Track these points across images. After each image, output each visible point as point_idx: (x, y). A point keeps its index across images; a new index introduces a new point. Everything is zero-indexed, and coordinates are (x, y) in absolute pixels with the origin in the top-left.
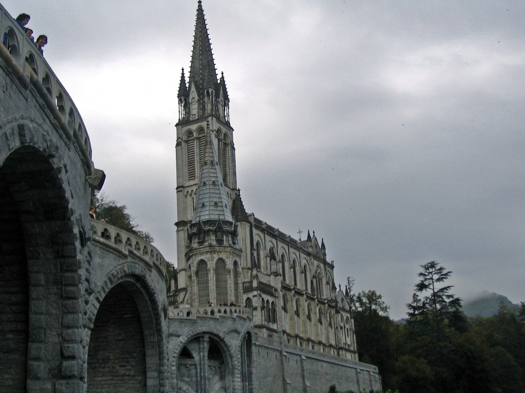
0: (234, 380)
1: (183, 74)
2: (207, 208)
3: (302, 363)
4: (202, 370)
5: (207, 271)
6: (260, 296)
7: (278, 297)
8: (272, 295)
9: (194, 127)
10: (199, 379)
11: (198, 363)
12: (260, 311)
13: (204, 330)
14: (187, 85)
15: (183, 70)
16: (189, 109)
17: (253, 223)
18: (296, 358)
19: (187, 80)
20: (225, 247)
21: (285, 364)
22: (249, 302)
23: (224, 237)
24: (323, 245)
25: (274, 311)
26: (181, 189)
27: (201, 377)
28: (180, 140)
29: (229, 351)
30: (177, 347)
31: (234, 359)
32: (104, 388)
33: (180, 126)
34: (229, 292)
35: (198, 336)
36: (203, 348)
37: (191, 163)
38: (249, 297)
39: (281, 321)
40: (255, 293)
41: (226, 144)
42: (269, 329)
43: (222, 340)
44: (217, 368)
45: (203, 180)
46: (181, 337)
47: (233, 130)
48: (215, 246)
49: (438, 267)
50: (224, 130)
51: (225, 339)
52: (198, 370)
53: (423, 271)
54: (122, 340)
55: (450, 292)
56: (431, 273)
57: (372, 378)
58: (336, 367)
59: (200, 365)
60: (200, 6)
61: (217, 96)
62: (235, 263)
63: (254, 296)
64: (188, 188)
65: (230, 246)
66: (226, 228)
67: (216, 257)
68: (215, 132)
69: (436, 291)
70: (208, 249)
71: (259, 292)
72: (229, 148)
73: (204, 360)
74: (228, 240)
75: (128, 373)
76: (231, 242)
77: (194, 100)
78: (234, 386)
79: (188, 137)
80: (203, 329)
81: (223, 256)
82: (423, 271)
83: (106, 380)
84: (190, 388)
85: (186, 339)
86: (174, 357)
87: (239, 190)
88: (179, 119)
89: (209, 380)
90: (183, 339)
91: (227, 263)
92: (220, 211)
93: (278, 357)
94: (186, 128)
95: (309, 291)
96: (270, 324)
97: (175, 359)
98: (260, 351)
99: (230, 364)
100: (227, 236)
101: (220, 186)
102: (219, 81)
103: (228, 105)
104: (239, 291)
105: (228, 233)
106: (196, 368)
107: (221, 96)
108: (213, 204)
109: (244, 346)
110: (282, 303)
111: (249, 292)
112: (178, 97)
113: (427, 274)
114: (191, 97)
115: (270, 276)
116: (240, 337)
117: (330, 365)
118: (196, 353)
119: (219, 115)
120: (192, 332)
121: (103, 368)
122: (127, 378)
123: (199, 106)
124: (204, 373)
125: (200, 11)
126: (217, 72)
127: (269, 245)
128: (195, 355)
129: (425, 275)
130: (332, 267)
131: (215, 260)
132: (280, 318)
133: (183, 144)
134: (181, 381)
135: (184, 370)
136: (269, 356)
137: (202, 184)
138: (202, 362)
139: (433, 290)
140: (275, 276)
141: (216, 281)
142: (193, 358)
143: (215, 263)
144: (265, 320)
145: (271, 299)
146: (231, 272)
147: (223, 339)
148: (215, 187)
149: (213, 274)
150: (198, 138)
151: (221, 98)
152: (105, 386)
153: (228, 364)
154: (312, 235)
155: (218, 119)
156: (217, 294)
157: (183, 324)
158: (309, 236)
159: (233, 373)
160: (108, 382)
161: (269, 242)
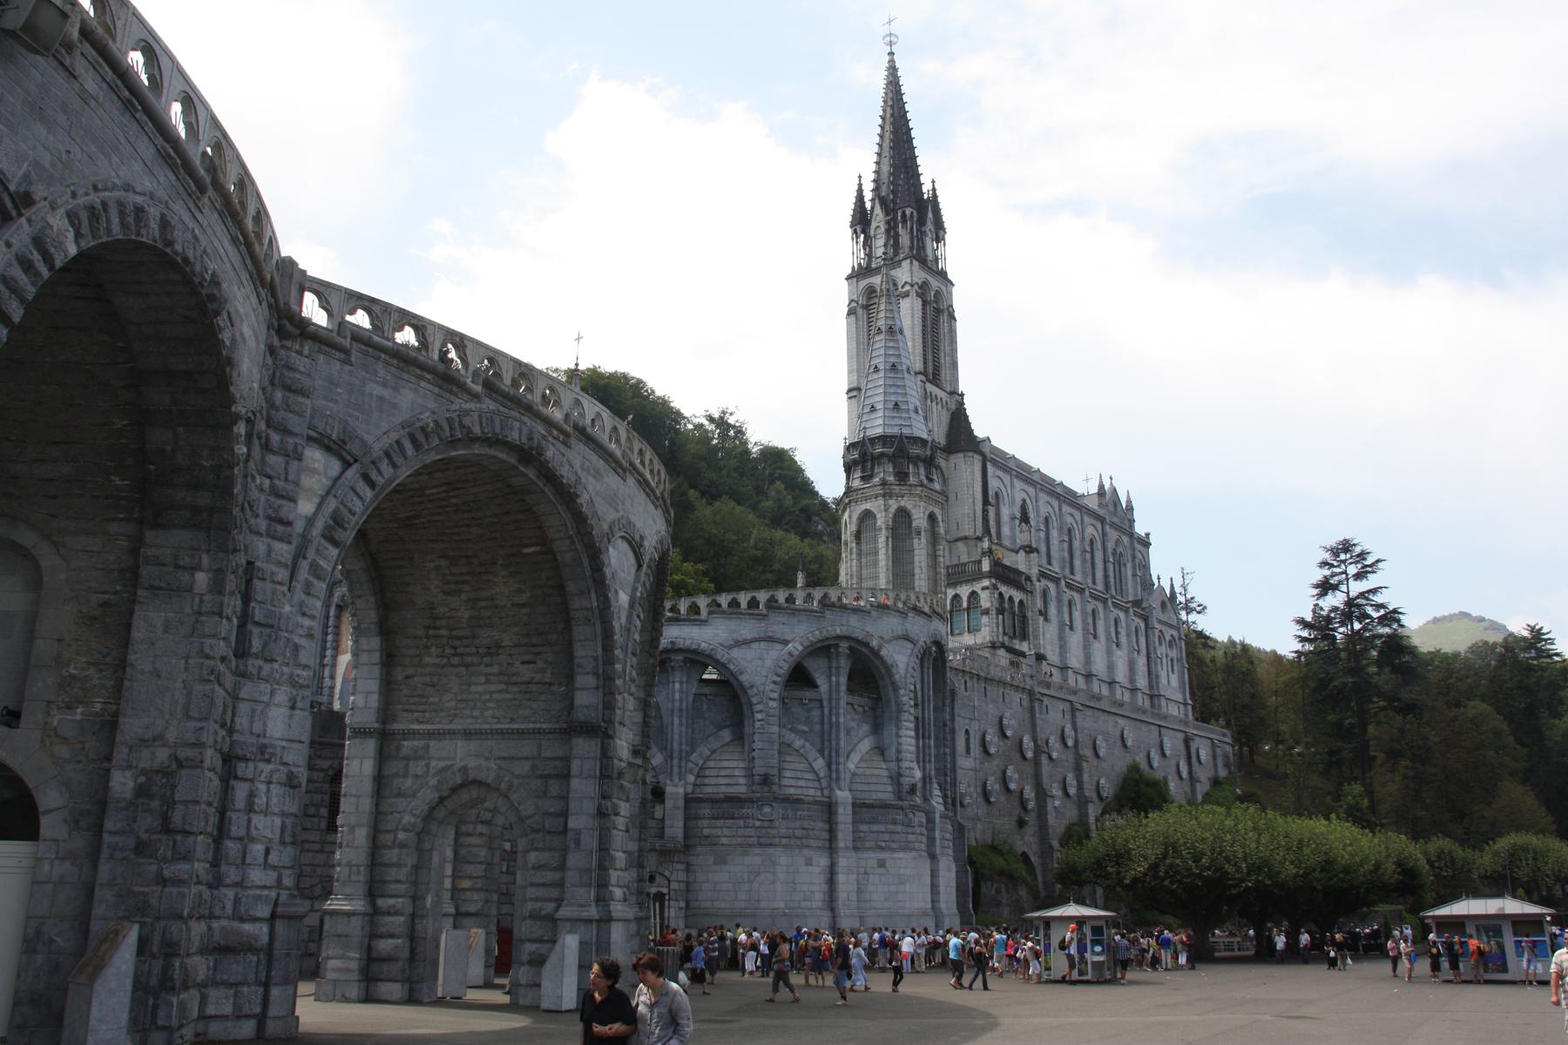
0: (900, 734)
1: (860, 185)
2: (880, 414)
3: (1073, 716)
4: (834, 711)
5: (876, 529)
6: (995, 587)
7: (1031, 592)
8: (1020, 587)
9: (876, 280)
10: (826, 727)
11: (825, 696)
12: (994, 616)
13: (838, 631)
14: (868, 205)
15: (860, 177)
16: (871, 247)
17: (989, 456)
18: (1061, 706)
19: (868, 195)
20: (911, 485)
21: (1037, 715)
22: (975, 599)
23: (911, 466)
24: (1129, 502)
25: (1024, 619)
26: (854, 393)
27: (830, 724)
28: (854, 304)
29: (891, 675)
30: (782, 663)
31: (902, 692)
32: (488, 709)
33: (855, 280)
34: (917, 571)
35: (826, 643)
36: (838, 668)
38: (975, 589)
39: (1036, 637)
40: (986, 583)
41: (938, 311)
42: (1010, 650)
43: (876, 653)
44: (867, 709)
45: (874, 362)
46: (790, 645)
47: (953, 285)
48: (891, 484)
49: (1358, 550)
50: (935, 283)
51: (883, 652)
52: (826, 711)
53: (1327, 556)
54: (524, 605)
55: (1378, 598)
56: (1344, 562)
57: (1218, 751)
58: (1143, 726)
59: (830, 700)
60: (892, 61)
61: (922, 222)
62: (932, 518)
63: (983, 589)
65: (922, 485)
66: (915, 451)
67: (893, 505)
68: (916, 287)
69: (1352, 594)
70: (879, 490)
71: (993, 581)
72: (944, 318)
73: (838, 691)
74: (918, 474)
75: (538, 677)
76: (923, 477)
78: (899, 744)
79: (869, 299)
80: (835, 630)
81: (906, 503)
82: (1327, 556)
83: (491, 693)
84: (807, 744)
85: (800, 648)
86: (774, 682)
87: (962, 395)
88: (853, 267)
89: (848, 732)
90: (796, 647)
91: (915, 516)
92: (905, 418)
93: (1026, 703)
94: (864, 283)
95: (1100, 586)
96: (1015, 641)
97: (777, 688)
98: (988, 688)
99: (893, 703)
100: (916, 465)
101: (905, 373)
102: (926, 196)
103: (944, 239)
104: (938, 570)
105: (916, 460)
106: (822, 707)
107: (929, 223)
108: (891, 406)
109: (928, 668)
110: (1039, 604)
111: (974, 580)
112: (851, 227)
113: (1335, 564)
114: (874, 225)
115: (1017, 552)
116: (916, 650)
117: (1133, 723)
118: (823, 677)
119: (927, 256)
120: (814, 635)
121: (487, 665)
122: (534, 688)
124: (838, 716)
125: (893, 70)
126: (922, 179)
127: (1019, 496)
128: (821, 681)
129: (1332, 566)
130: (1145, 543)
131: (892, 510)
132: (1035, 630)
133: (860, 311)
134: (791, 730)
135: (797, 710)
136: (1007, 700)
137: (872, 370)
138: (834, 696)
139: (1348, 593)
140: (1026, 552)
141: (893, 550)
142: (816, 686)
143: (891, 516)
144: (1005, 634)
145: (1018, 596)
146: (923, 533)
147: (879, 650)
148: (896, 373)
149: (887, 538)
151: (930, 226)
152: (489, 705)
153: (888, 702)
154: (1107, 487)
155: (923, 262)
156: (893, 574)
157: (796, 619)
158: (1101, 487)
159: (899, 720)
160: (495, 696)
161: (1019, 491)
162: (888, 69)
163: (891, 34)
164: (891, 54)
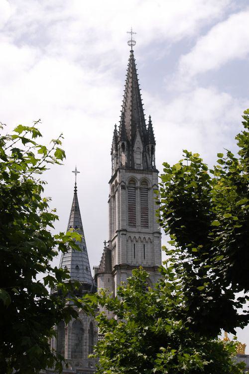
9: (139, 176)
33: (124, 171)
37: (131, 209)
60: (132, 56)
64: (130, 233)
77: (138, 150)
79: (129, 183)
94: (130, 175)
114: (136, 146)
123: (143, 157)
125: (132, 60)
150: (140, 188)
162: (130, 60)
163: (132, 41)
164: (132, 51)
